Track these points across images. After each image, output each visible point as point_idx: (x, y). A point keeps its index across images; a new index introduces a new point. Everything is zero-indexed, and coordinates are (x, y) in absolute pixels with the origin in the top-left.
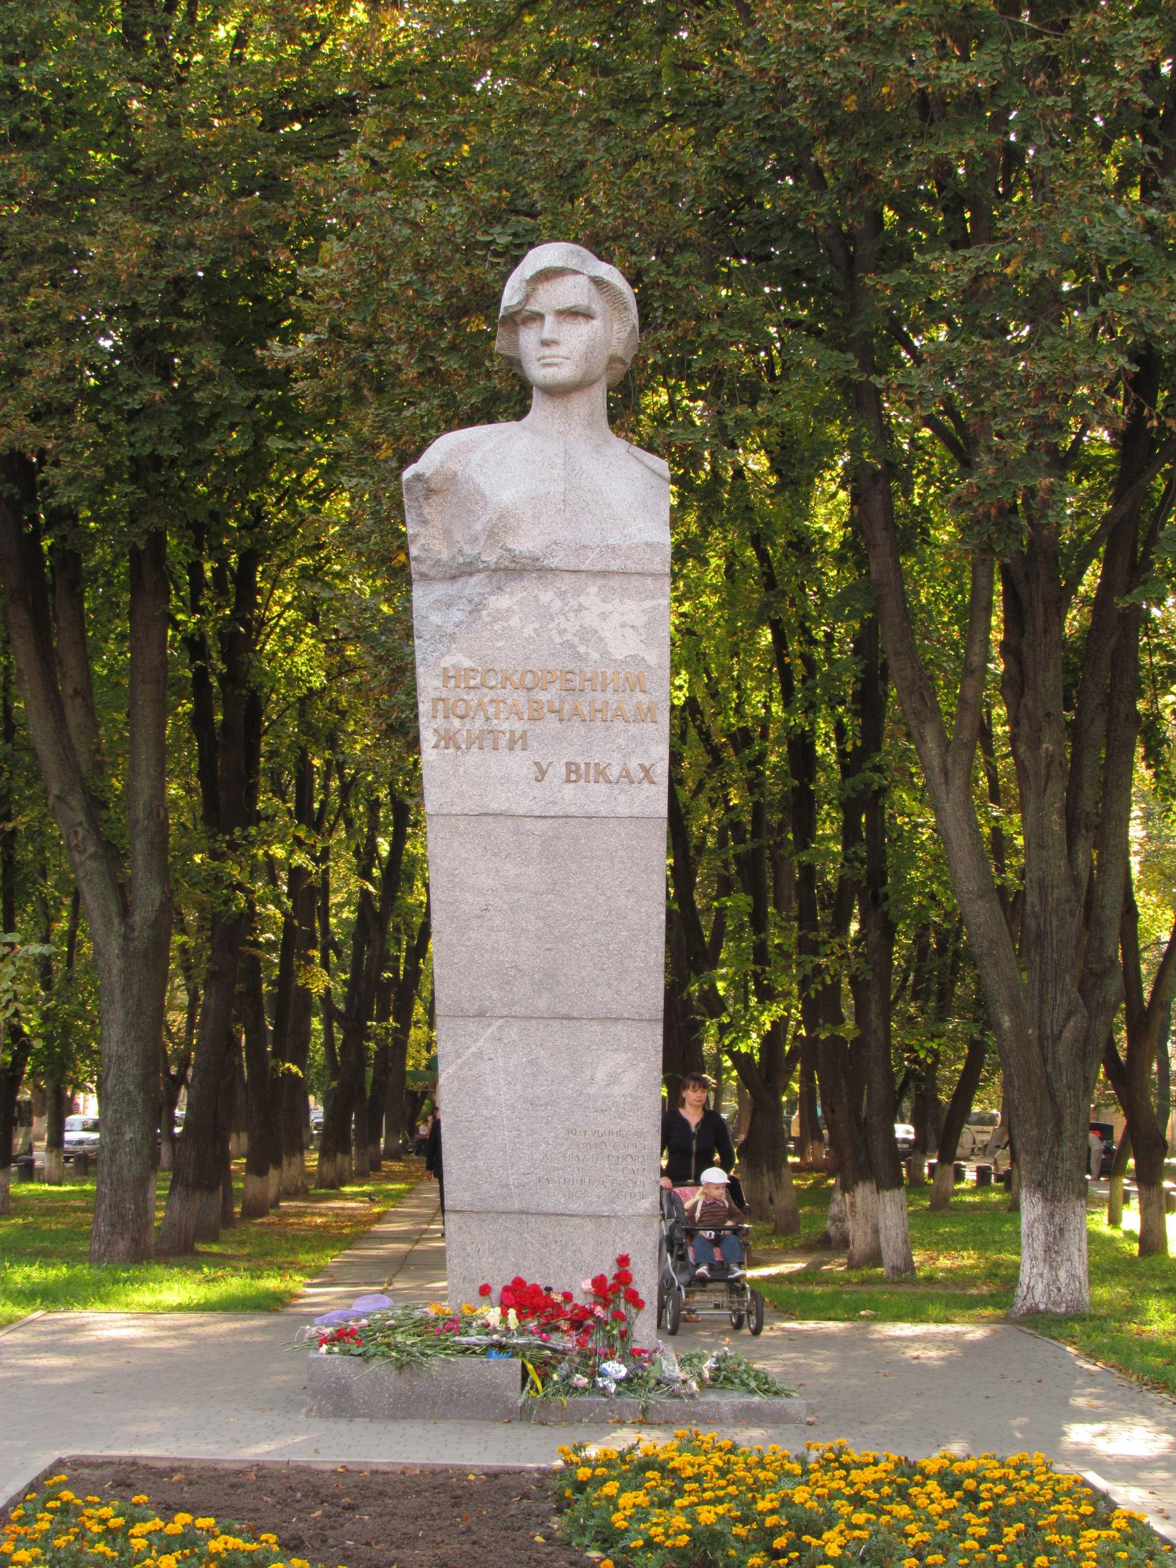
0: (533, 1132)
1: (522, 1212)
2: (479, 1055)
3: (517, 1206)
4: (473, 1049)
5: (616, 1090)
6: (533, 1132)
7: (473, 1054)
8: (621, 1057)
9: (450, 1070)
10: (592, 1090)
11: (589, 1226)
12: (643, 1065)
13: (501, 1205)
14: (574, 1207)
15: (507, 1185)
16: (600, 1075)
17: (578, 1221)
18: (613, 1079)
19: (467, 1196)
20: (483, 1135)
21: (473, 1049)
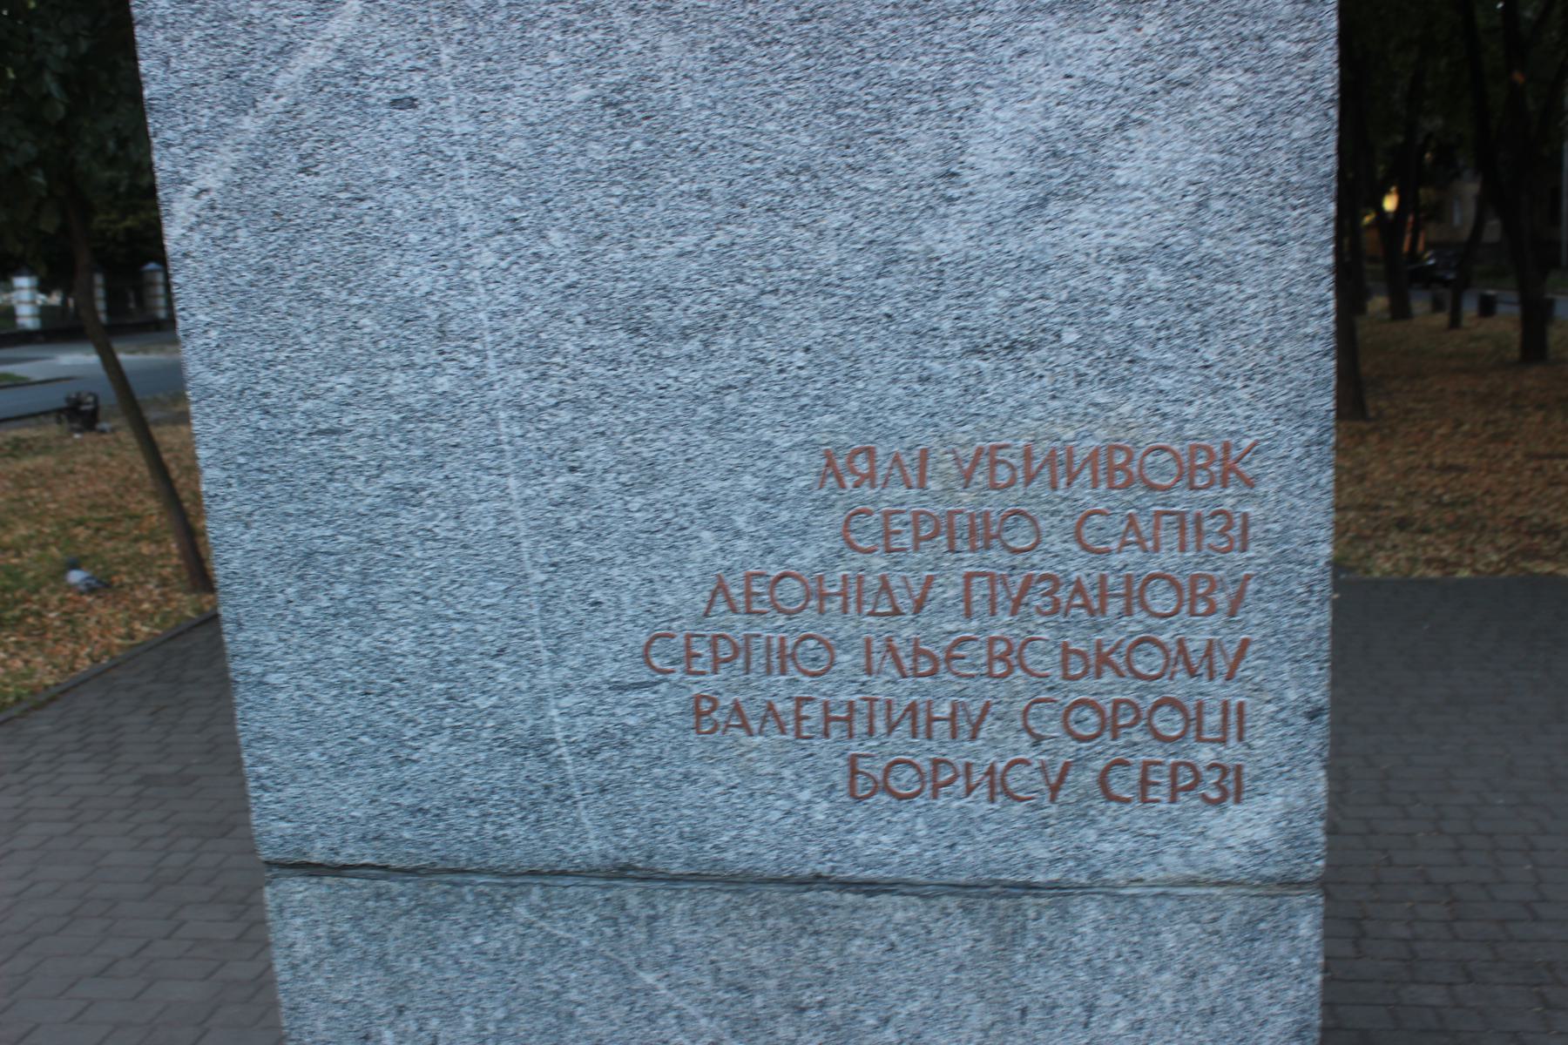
0: (651, 475)
1: (622, 872)
2: (346, 83)
3: (594, 846)
4: (312, 57)
5: (1085, 228)
6: (651, 475)
7: (316, 81)
8: (1102, 46)
9: (212, 176)
10: (950, 238)
11: (961, 936)
12: (1227, 84)
13: (522, 841)
14: (885, 839)
15: (539, 746)
16: (996, 145)
17: (897, 910)
18: (1065, 170)
19: (353, 797)
20: (403, 497)
21: (312, 57)
